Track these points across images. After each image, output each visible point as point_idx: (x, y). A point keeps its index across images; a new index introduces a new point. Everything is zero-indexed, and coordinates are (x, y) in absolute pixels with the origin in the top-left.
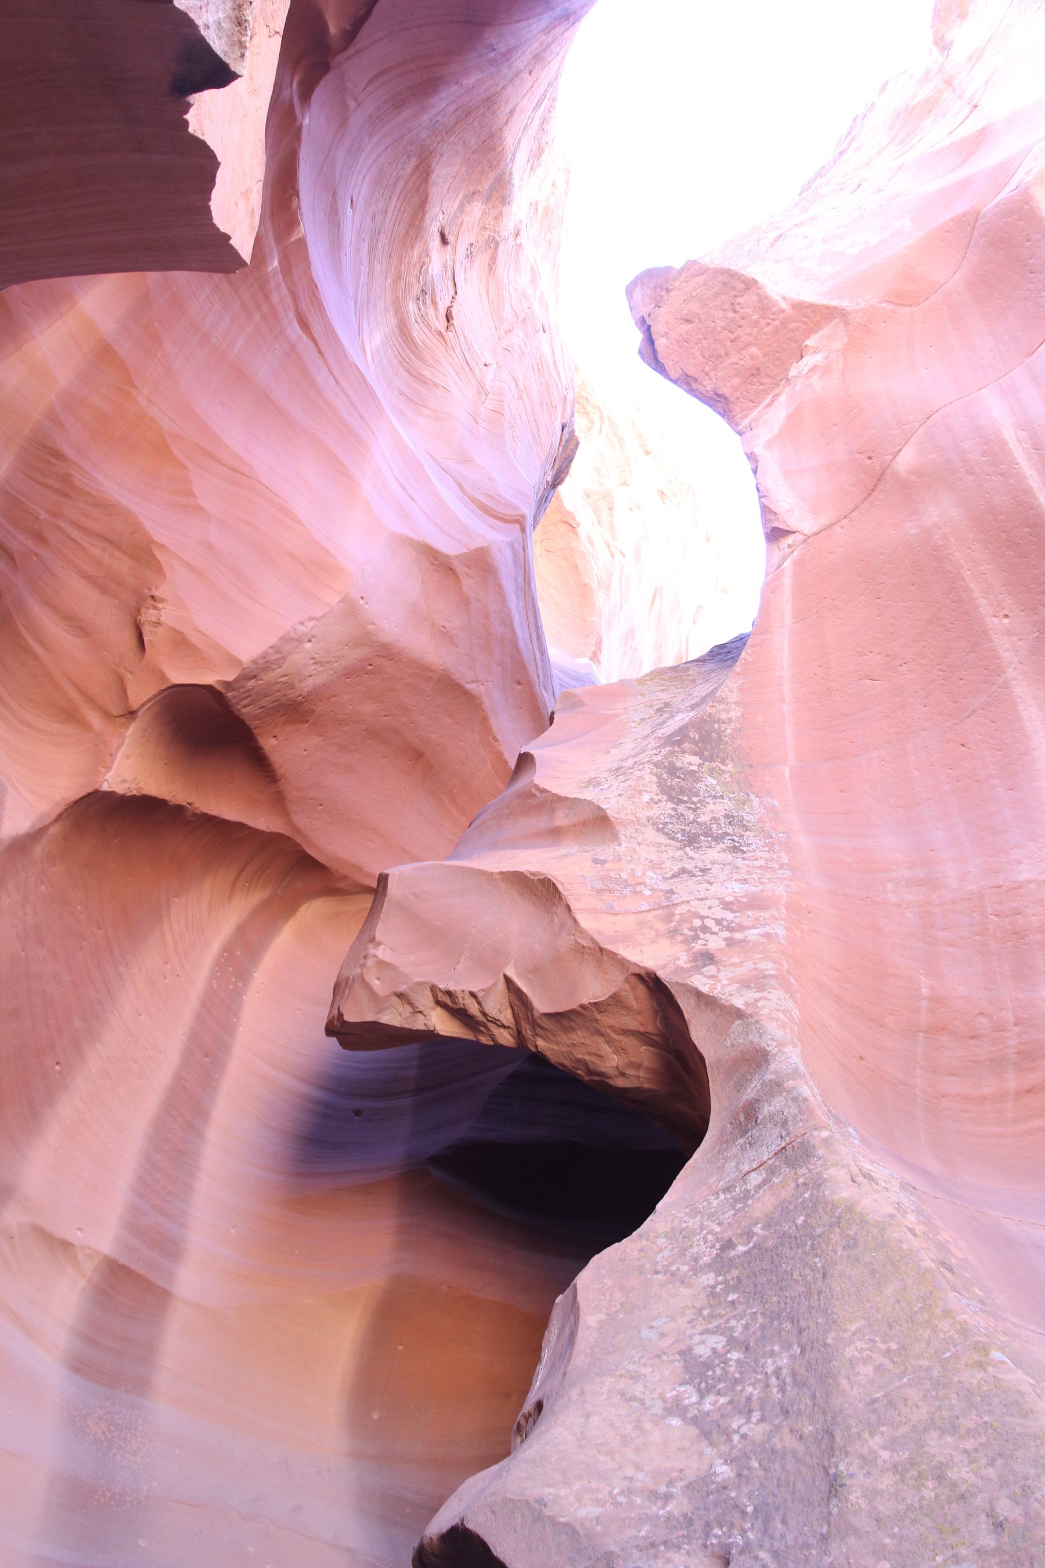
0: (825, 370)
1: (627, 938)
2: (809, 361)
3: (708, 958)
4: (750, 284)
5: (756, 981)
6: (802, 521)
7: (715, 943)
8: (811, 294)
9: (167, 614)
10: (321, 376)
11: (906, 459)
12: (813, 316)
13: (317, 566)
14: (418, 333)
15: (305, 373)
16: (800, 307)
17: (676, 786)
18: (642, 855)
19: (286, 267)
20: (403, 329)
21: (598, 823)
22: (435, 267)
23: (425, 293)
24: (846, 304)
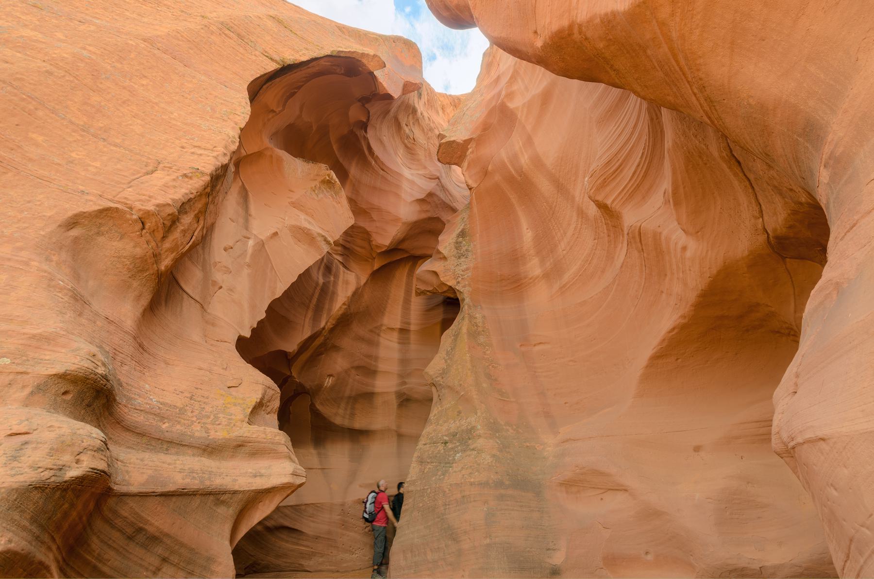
0: (472, 152)
1: (448, 281)
2: (470, 150)
3: (458, 282)
4: (454, 141)
5: (464, 287)
6: (474, 185)
7: (460, 279)
8: (467, 138)
9: (374, 243)
10: (389, 178)
11: (490, 168)
12: (467, 142)
13: (397, 219)
14: (409, 145)
15: (386, 179)
16: (465, 141)
17: (458, 245)
18: (451, 263)
19: (376, 161)
20: (406, 146)
21: (445, 258)
22: (407, 131)
23: (408, 137)
24: (474, 136)
